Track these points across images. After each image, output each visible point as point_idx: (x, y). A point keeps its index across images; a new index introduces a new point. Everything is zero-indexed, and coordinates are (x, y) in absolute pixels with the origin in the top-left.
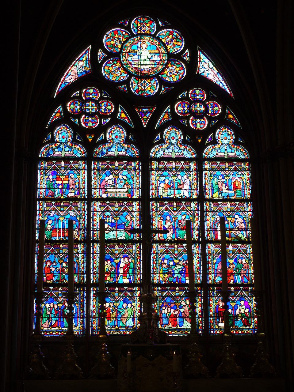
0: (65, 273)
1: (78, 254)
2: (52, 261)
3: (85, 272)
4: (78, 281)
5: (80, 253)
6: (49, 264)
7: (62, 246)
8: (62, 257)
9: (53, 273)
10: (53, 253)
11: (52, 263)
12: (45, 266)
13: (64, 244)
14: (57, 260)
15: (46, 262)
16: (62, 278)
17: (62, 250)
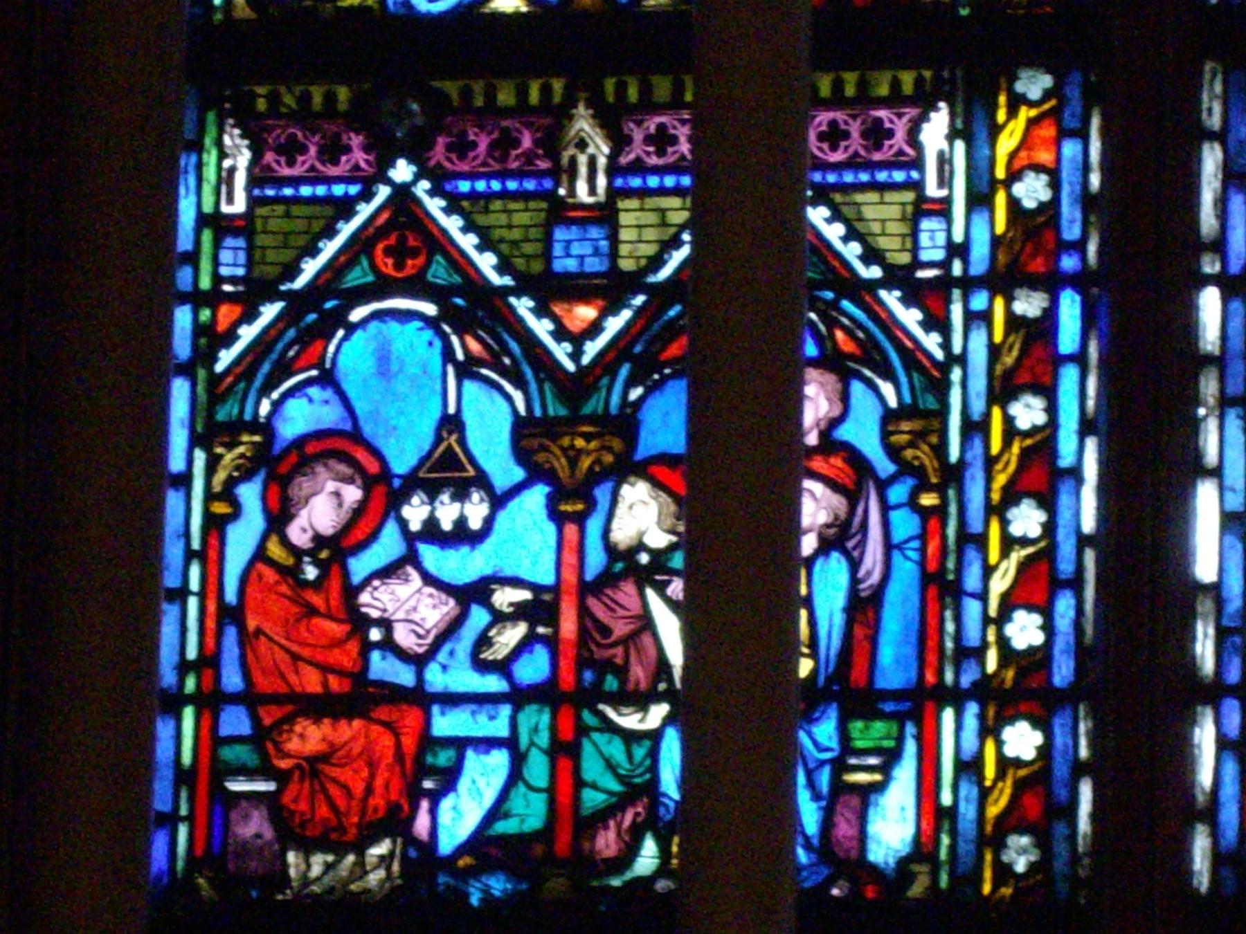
0: (641, 701)
1: (931, 297)
2: (403, 456)
3: (1063, 671)
4: (922, 851)
5: (968, 284)
6: (323, 508)
7: (601, 148)
8: (607, 362)
9: (422, 699)
10: (417, 286)
11: (384, 492)
12: (260, 555)
13: (648, 106)
14: (489, 422)
15: (285, 469)
16: (592, 799)
17: (605, 215)
